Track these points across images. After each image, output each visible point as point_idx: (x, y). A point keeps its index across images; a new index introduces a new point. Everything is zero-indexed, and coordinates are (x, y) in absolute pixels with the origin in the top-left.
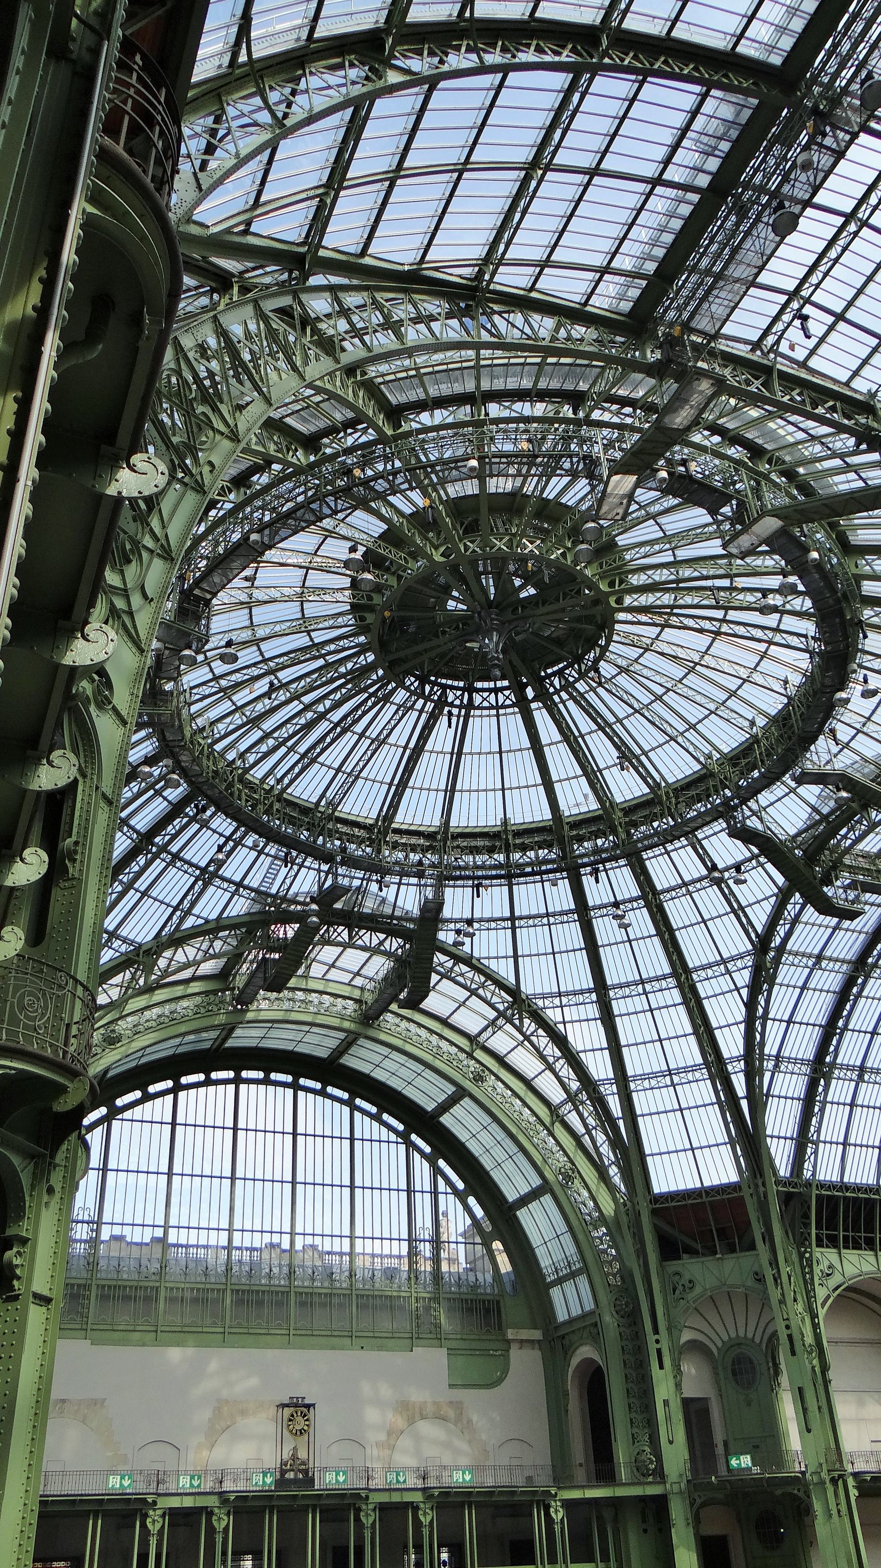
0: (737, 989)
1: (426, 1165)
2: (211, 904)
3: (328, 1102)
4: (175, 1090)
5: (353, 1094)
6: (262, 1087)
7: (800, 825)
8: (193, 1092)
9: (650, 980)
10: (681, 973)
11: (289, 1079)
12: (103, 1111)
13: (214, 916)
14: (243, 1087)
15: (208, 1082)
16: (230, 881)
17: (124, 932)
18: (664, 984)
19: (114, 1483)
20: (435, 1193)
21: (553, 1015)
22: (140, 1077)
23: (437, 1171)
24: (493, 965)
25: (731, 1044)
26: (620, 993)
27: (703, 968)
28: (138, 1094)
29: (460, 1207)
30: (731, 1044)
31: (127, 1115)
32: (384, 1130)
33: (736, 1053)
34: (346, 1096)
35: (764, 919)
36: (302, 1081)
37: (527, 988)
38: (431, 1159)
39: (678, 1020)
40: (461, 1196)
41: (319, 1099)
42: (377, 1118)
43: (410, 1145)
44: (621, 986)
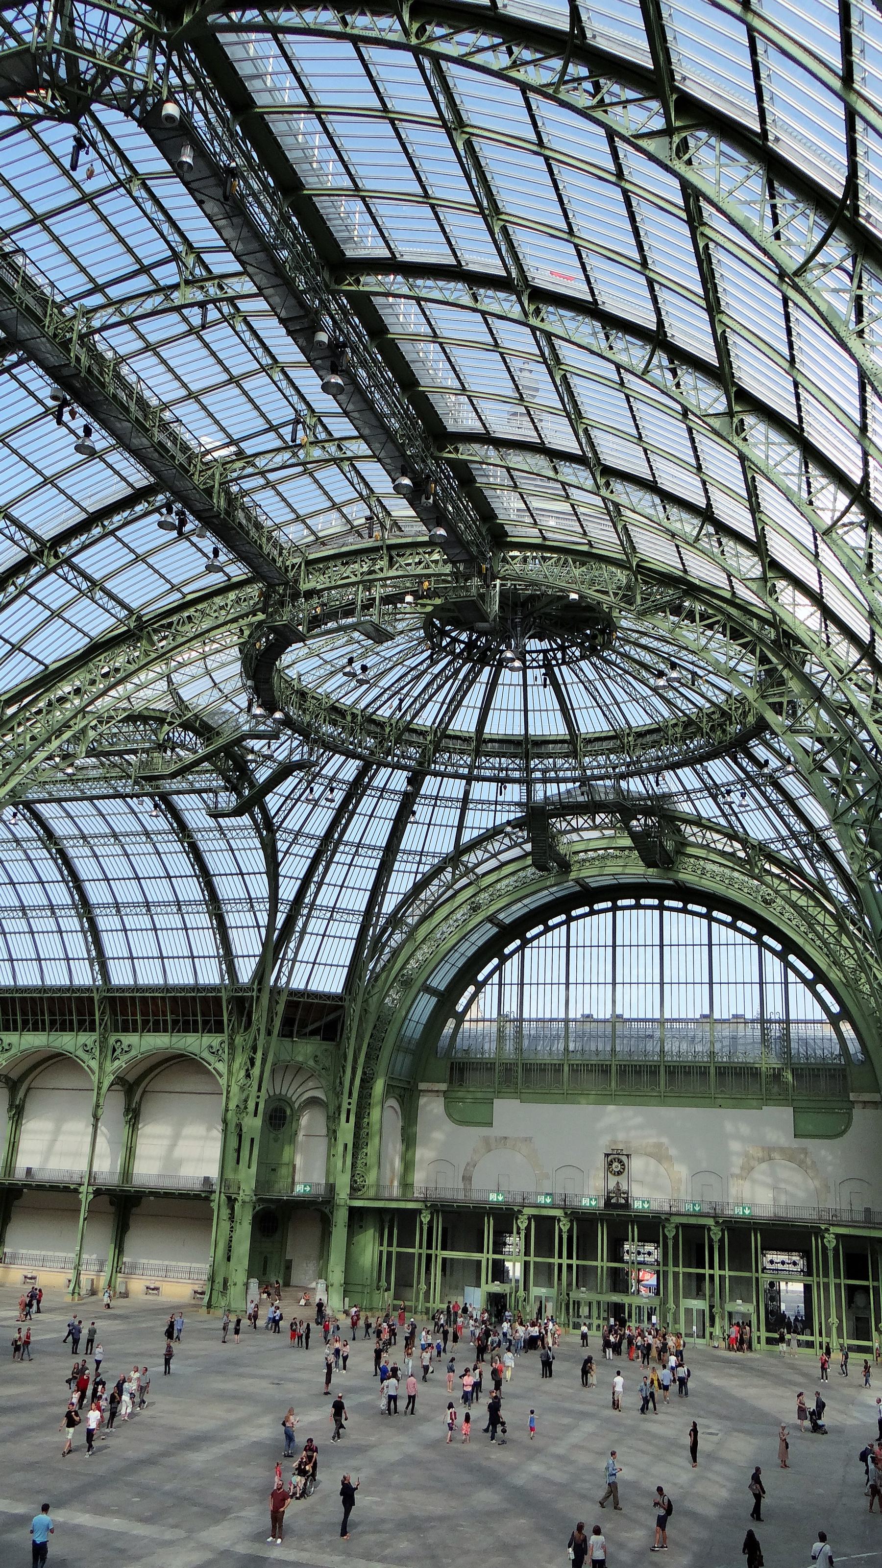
1: (777, 961)
2: (479, 821)
3: (689, 917)
4: (567, 922)
5: (710, 909)
6: (634, 912)
8: (581, 921)
11: (656, 902)
12: (518, 942)
13: (490, 825)
14: (619, 914)
15: (592, 912)
16: (489, 802)
17: (430, 847)
19: (493, 1197)
20: (786, 983)
22: (540, 916)
23: (788, 965)
28: (541, 928)
29: (809, 994)
31: (535, 943)
32: (738, 935)
34: (704, 910)
36: (667, 903)
38: (781, 956)
40: (810, 985)
41: (682, 915)
42: (732, 926)
43: (762, 945)
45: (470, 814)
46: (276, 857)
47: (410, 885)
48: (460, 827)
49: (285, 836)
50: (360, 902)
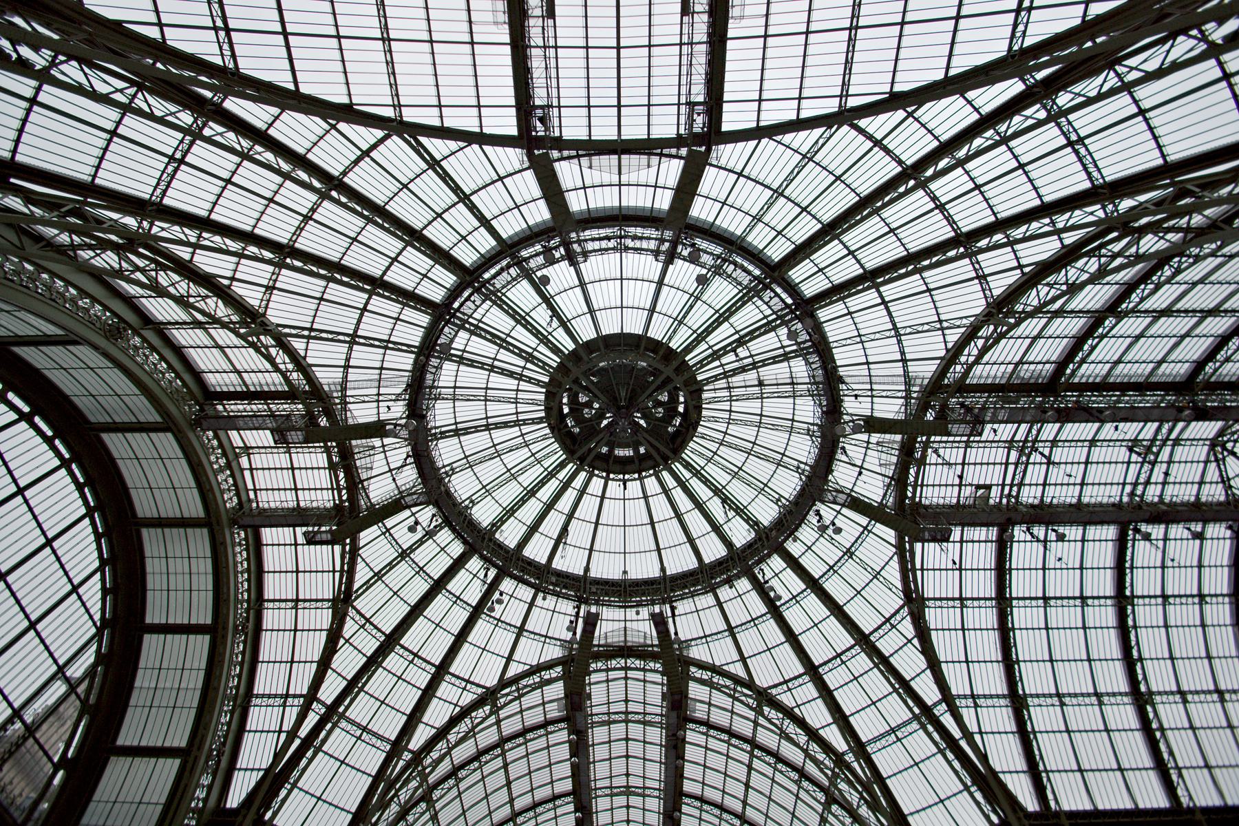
0: (909, 641)
2: (530, 653)
7: (881, 492)
9: (844, 652)
10: (864, 641)
13: (535, 663)
18: (853, 652)
21: (787, 700)
24: (730, 669)
25: (928, 691)
26: (826, 668)
27: (876, 630)
30: (928, 691)
33: (936, 699)
35: (898, 575)
37: (762, 681)
39: (877, 683)
44: (825, 663)
45: (523, 640)
46: (337, 643)
47: (447, 718)
48: (509, 659)
49: (358, 617)
50: (391, 726)
